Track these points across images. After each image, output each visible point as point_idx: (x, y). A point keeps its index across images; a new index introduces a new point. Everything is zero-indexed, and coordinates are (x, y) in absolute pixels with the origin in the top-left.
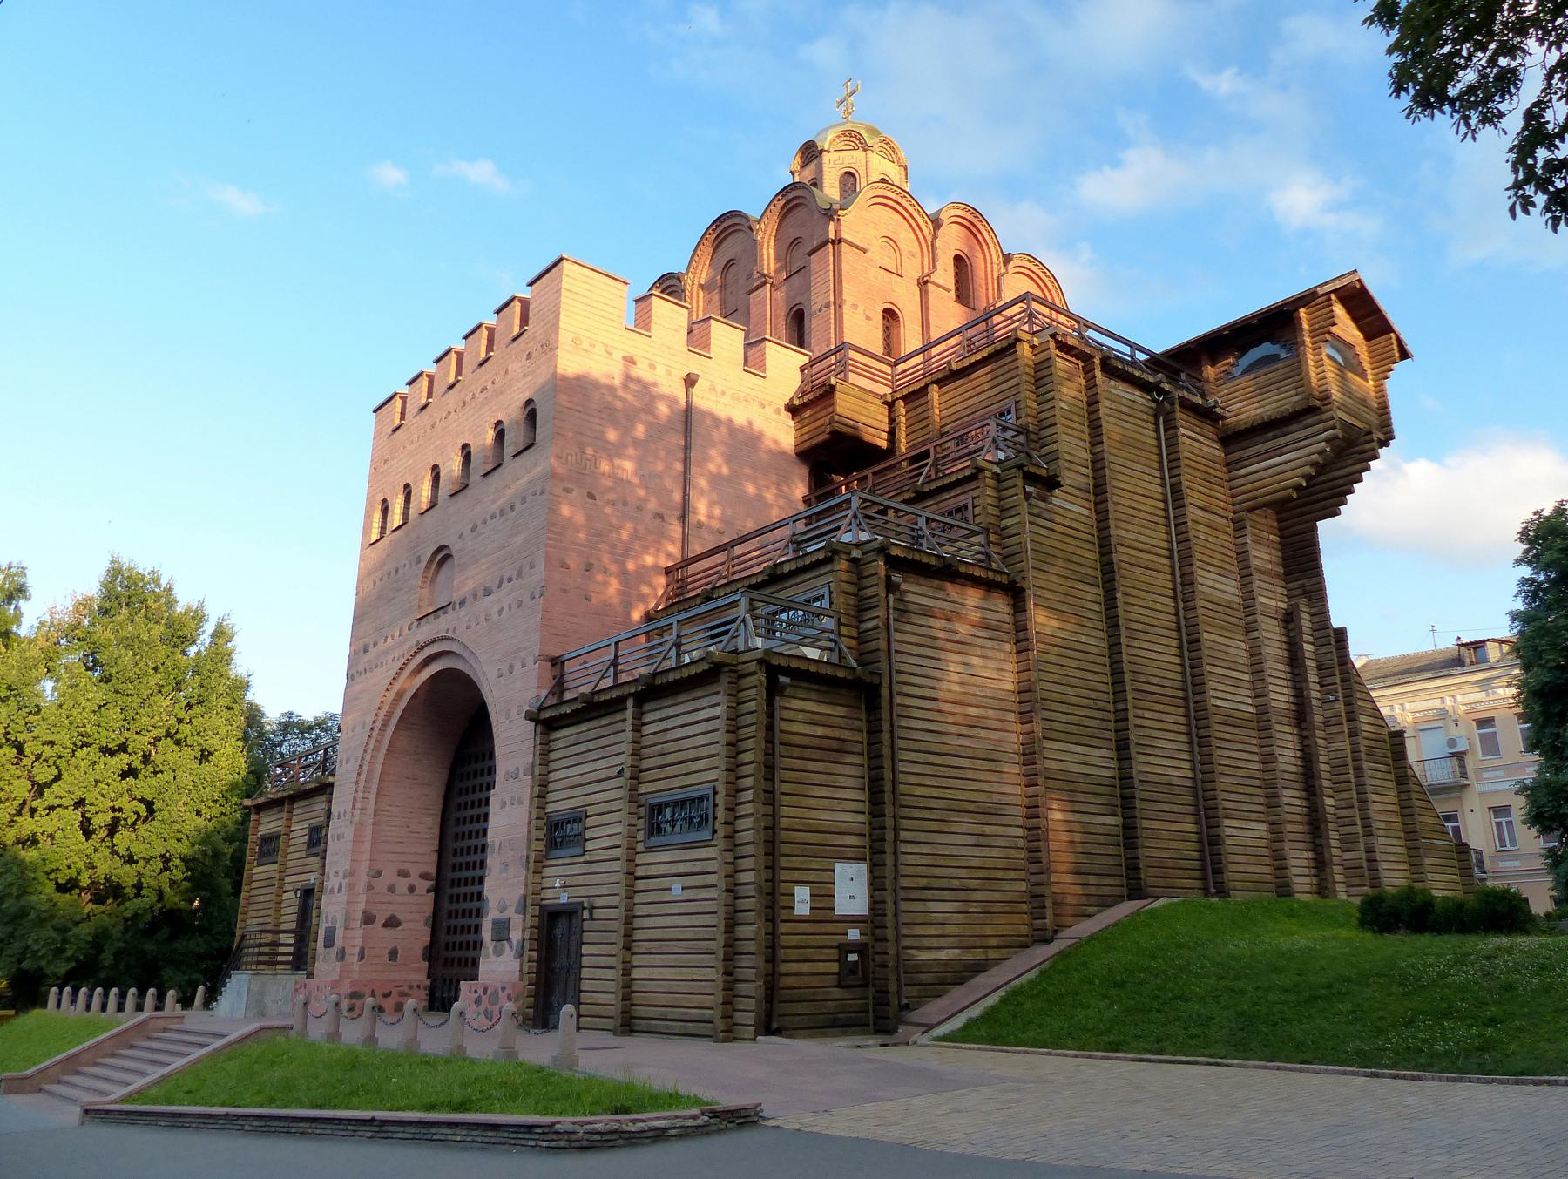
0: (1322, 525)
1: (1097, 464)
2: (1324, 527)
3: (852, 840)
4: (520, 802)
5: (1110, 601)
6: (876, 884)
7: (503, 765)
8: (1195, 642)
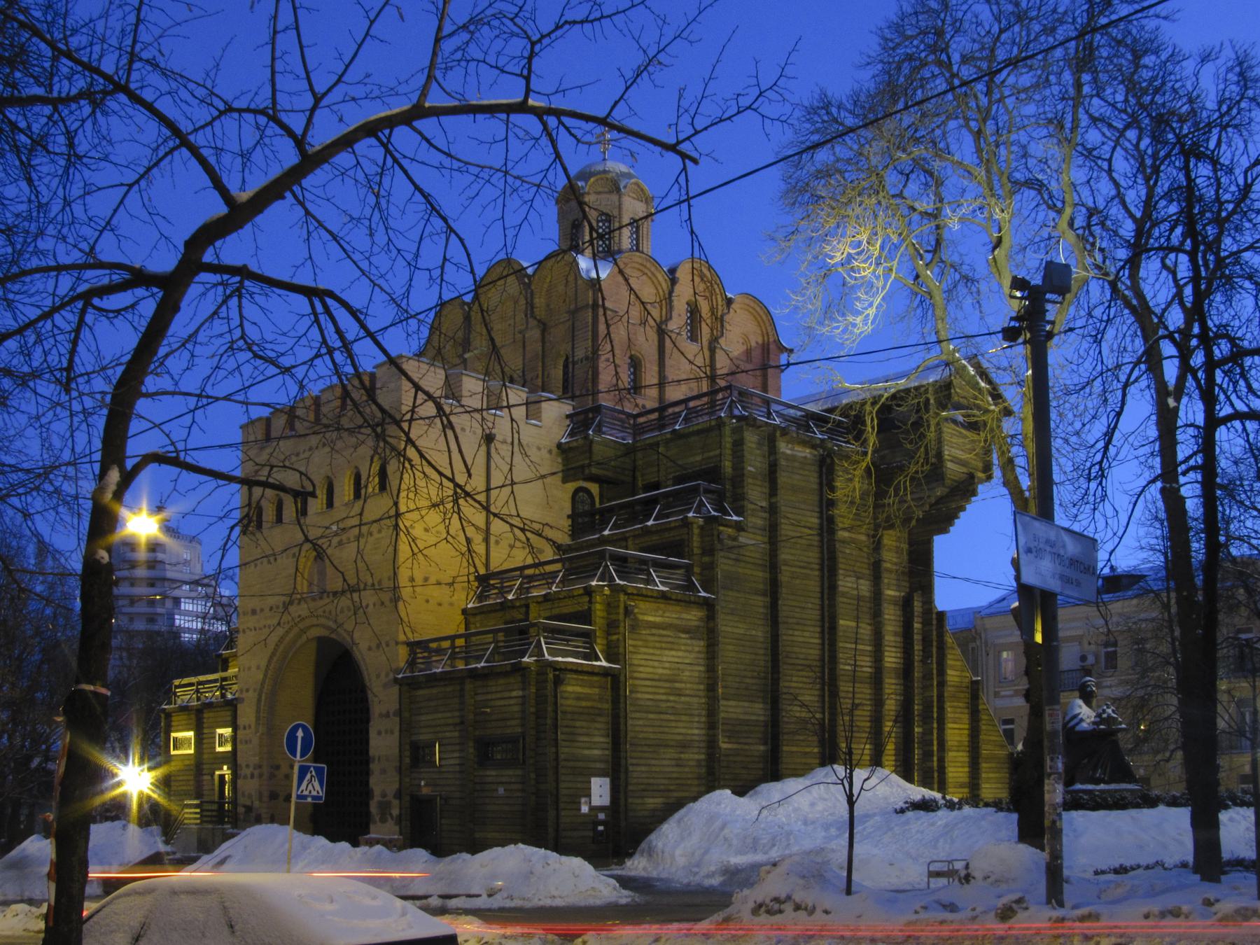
0: (936, 538)
1: (773, 510)
2: (936, 538)
3: (598, 765)
4: (392, 732)
5: (774, 607)
6: (615, 790)
7: (376, 709)
8: (833, 628)
